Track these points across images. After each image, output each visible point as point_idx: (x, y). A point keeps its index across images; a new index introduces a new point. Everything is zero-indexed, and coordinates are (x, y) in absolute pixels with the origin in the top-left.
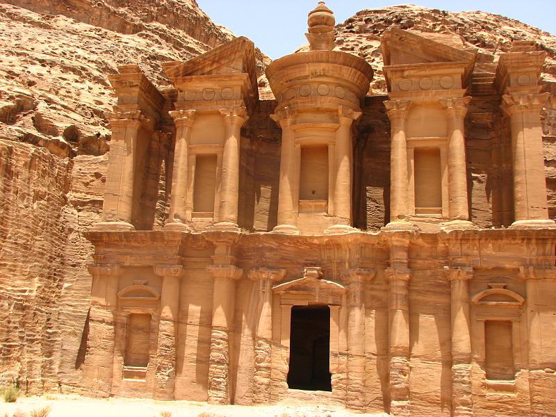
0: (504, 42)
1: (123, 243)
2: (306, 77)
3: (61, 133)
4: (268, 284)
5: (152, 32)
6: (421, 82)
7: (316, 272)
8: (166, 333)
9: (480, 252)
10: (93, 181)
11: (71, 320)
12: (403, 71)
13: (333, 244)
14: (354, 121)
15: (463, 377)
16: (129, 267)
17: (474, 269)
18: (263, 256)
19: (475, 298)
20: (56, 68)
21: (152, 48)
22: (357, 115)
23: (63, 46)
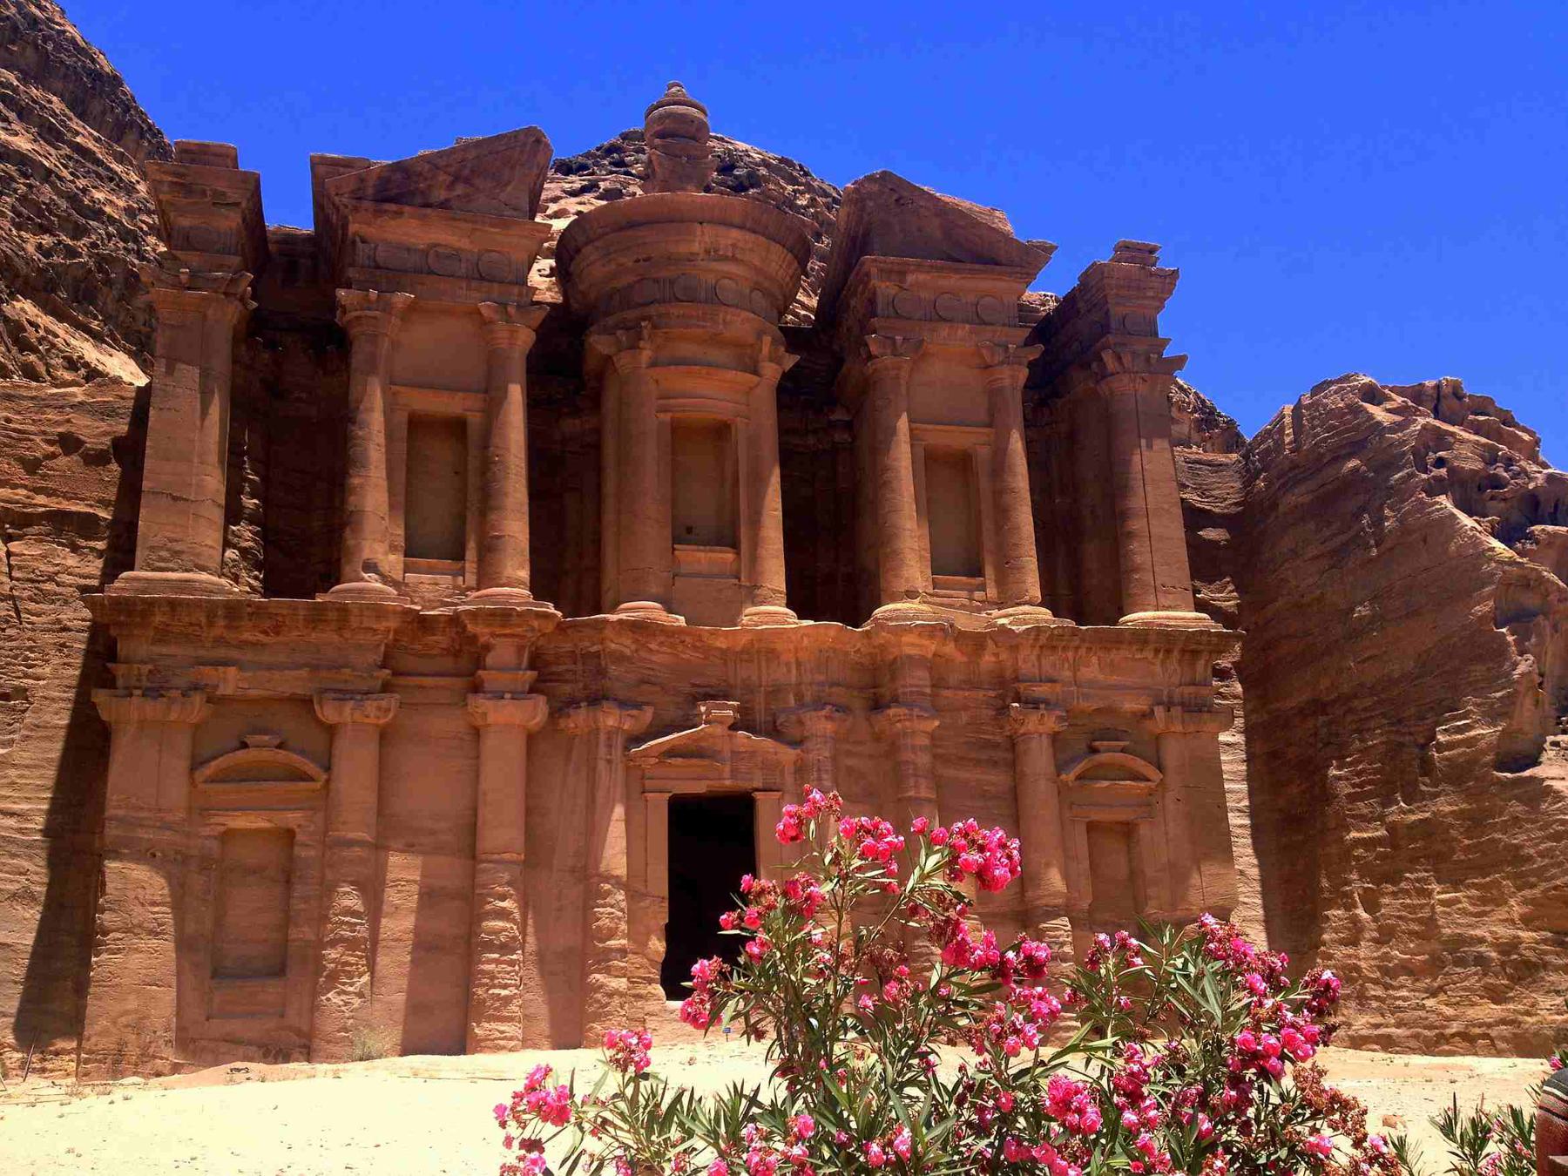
2: (691, 258)
4: (619, 741)
9: (1075, 676)
10: (53, 456)
11: (13, 856)
12: (902, 274)
18: (601, 673)
22: (790, 361)
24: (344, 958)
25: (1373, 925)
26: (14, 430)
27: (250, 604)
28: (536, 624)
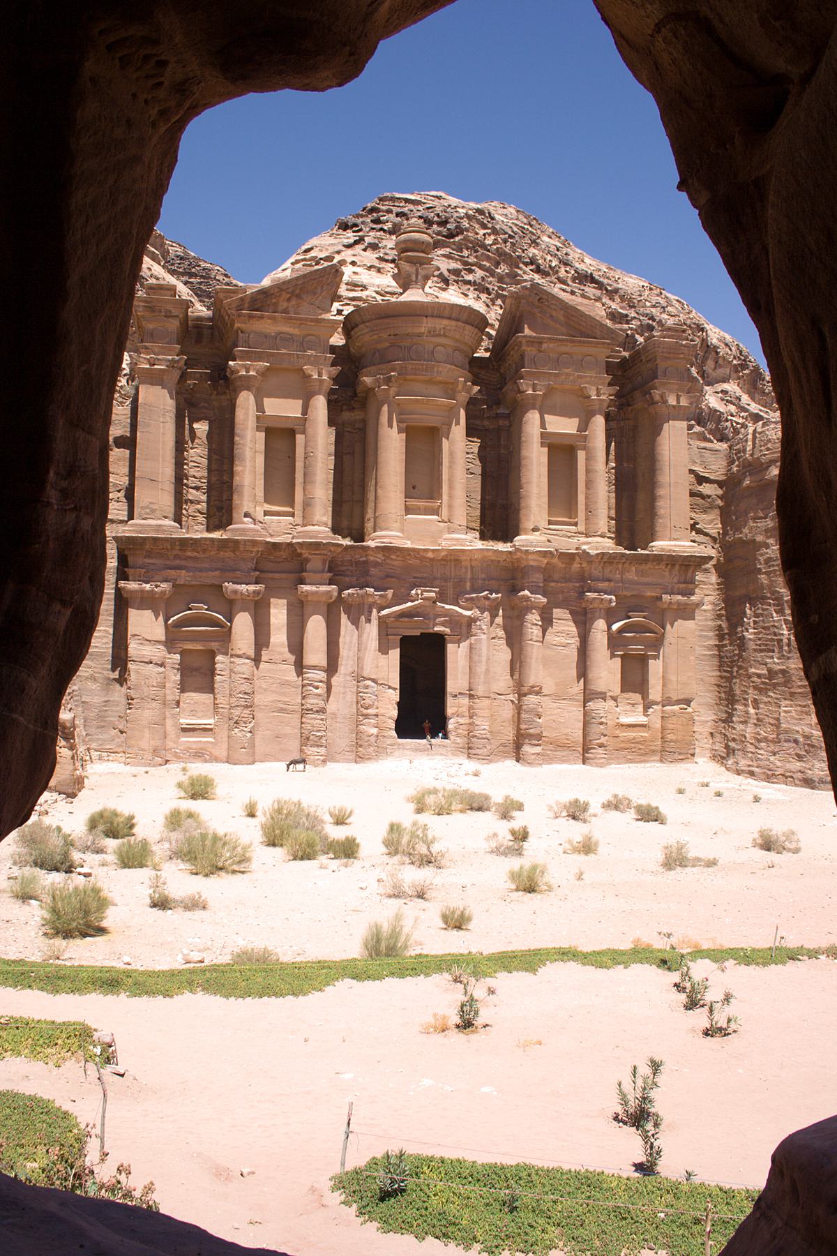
0: (553, 264)
2: (420, 335)
6: (560, 359)
7: (433, 595)
8: (244, 676)
12: (541, 343)
13: (453, 558)
15: (601, 718)
16: (184, 585)
18: (367, 573)
19: (615, 627)
24: (242, 715)
25: (755, 717)
28: (332, 549)
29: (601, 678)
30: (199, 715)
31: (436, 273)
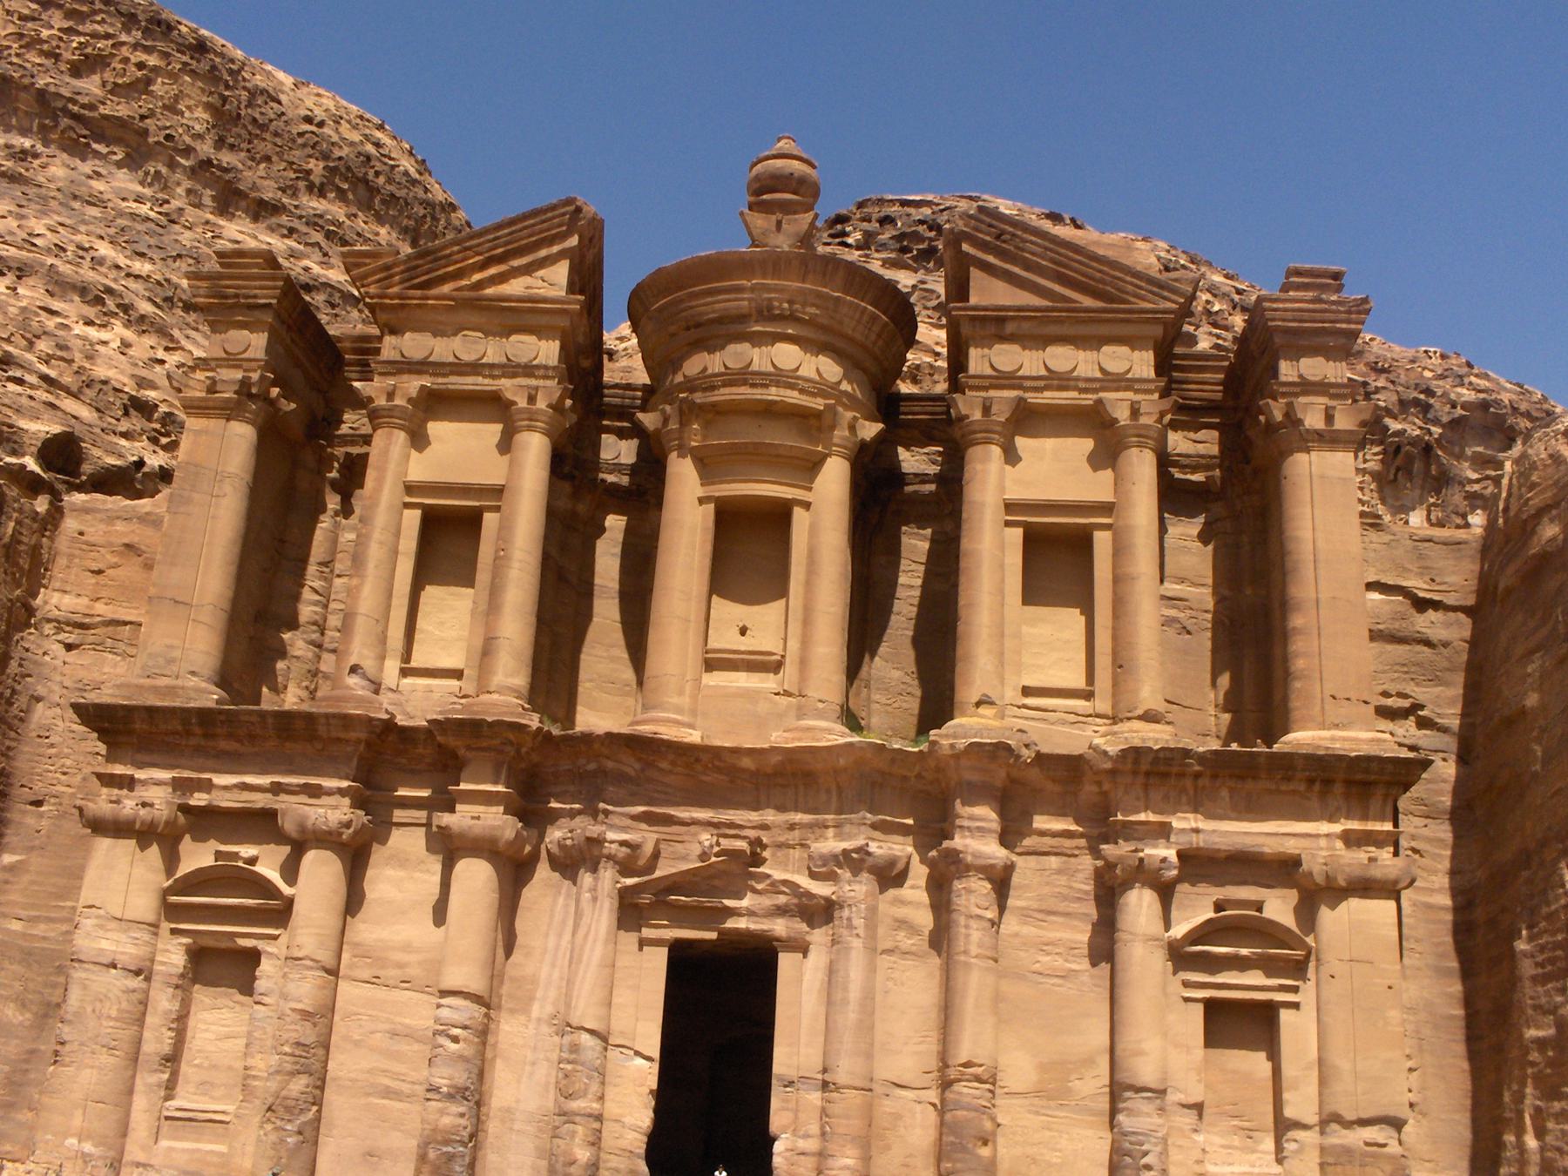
0: (1216, 308)
1: (193, 741)
2: (742, 318)
3: (34, 449)
4: (608, 874)
5: (307, 224)
7: (742, 845)
8: (300, 1006)
14: (863, 441)
15: (1146, 1154)
17: (1180, 854)
19: (1179, 930)
20: (31, 281)
21: (306, 263)
22: (870, 430)
23: (60, 229)
24: (284, 1093)
26: (87, 543)
27: (221, 712)
28: (511, 736)
29: (1141, 1053)
30: (218, 1093)
31: (934, 303)
